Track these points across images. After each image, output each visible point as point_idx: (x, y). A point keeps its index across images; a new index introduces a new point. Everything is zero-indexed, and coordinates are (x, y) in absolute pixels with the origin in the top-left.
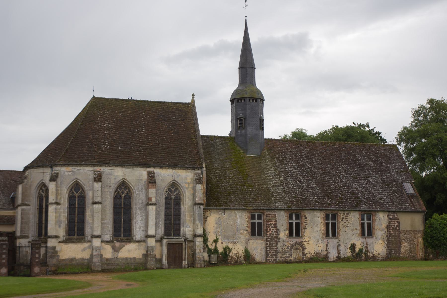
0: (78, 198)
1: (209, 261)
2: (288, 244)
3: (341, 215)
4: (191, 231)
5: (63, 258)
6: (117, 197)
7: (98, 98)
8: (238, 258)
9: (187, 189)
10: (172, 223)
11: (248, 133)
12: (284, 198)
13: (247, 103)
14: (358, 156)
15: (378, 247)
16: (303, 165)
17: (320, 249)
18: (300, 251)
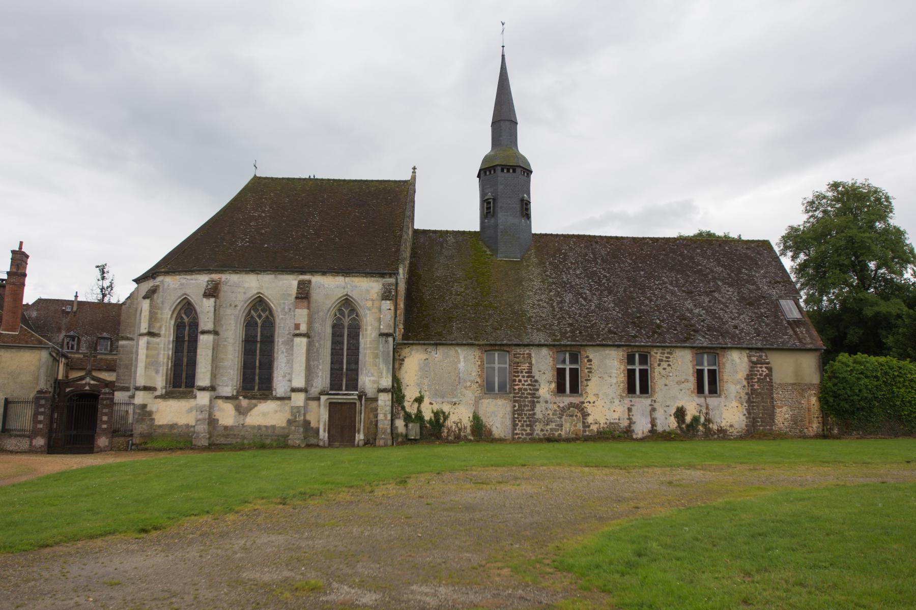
0: (190, 326)
1: (407, 435)
2: (555, 407)
3: (656, 355)
4: (374, 382)
5: (161, 423)
6: (250, 324)
7: (260, 178)
8: (460, 430)
9: (369, 309)
10: (344, 369)
11: (499, 221)
12: (551, 326)
13: (504, 176)
14: (698, 258)
15: (730, 412)
16: (595, 273)
17: (616, 416)
18: (578, 420)
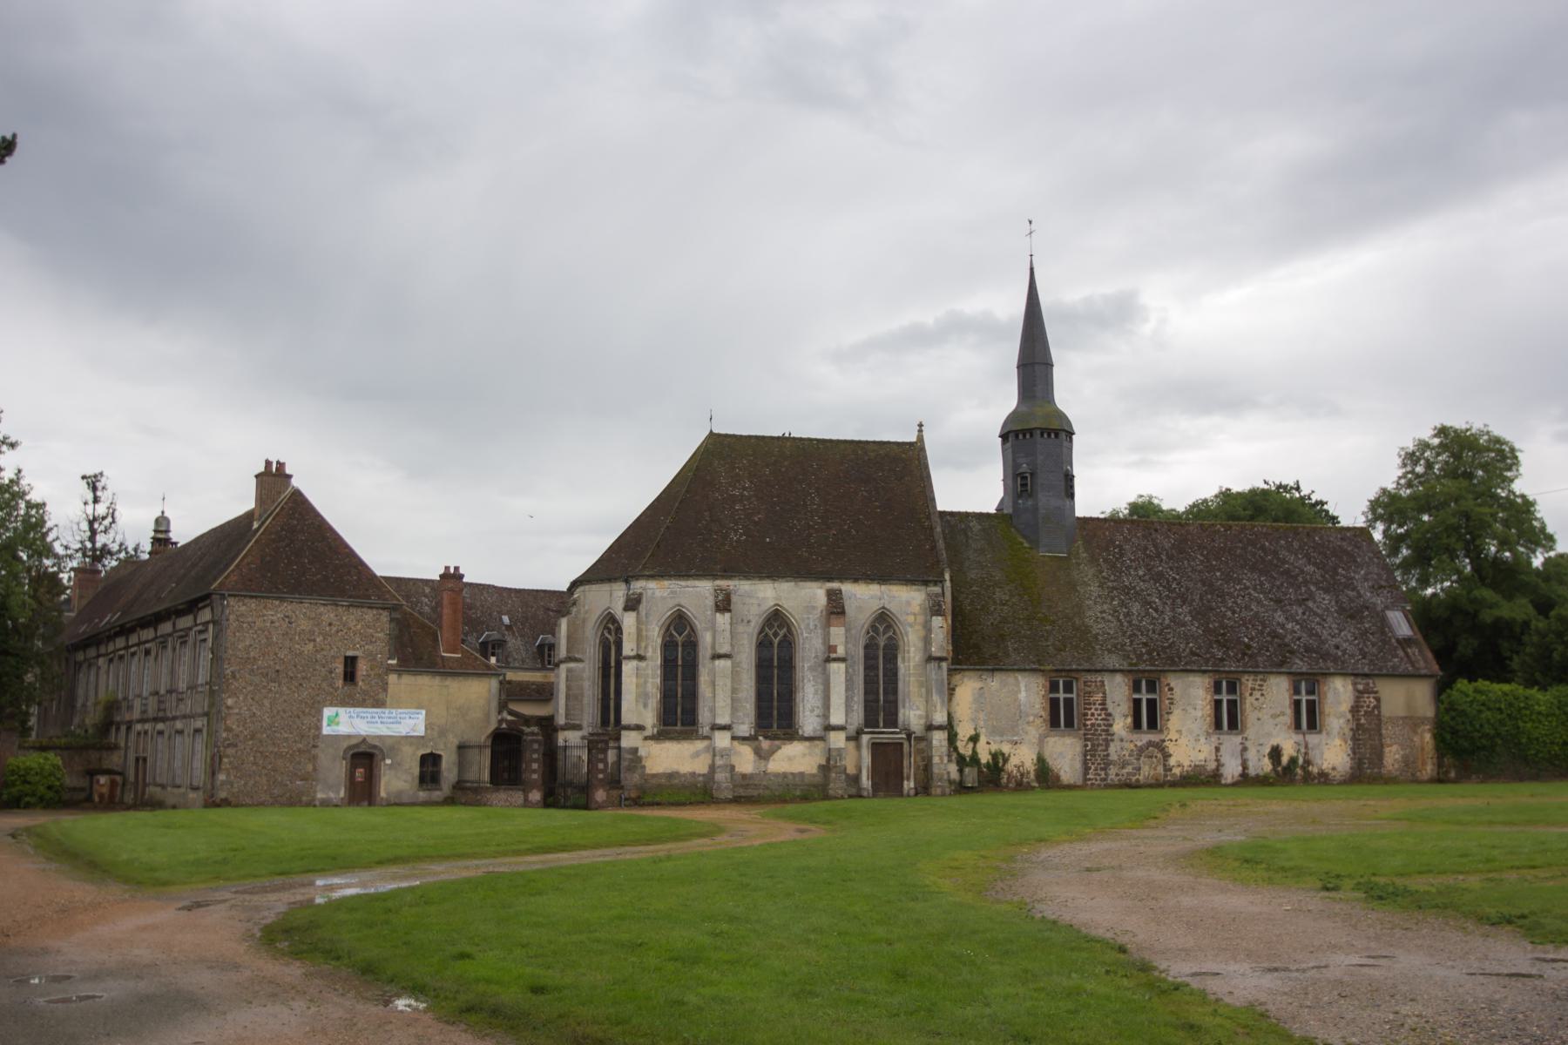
3: (1248, 682)
4: (920, 717)
6: (763, 644)
7: (719, 435)
10: (880, 700)
13: (1037, 441)
14: (1283, 553)
15: (1333, 753)
16: (1161, 574)
17: (1202, 756)
